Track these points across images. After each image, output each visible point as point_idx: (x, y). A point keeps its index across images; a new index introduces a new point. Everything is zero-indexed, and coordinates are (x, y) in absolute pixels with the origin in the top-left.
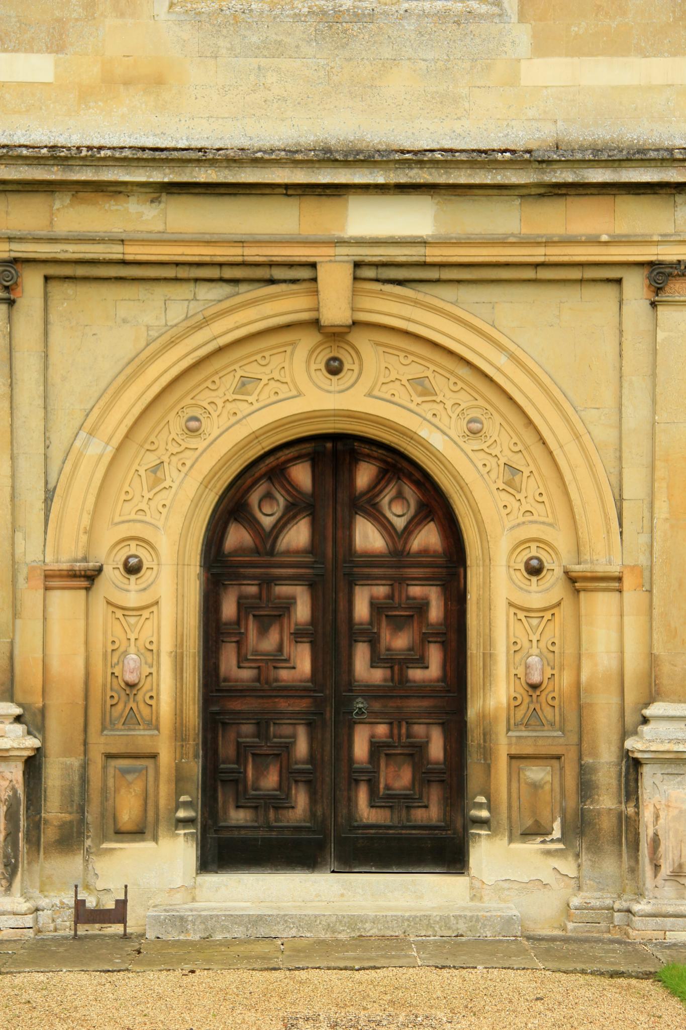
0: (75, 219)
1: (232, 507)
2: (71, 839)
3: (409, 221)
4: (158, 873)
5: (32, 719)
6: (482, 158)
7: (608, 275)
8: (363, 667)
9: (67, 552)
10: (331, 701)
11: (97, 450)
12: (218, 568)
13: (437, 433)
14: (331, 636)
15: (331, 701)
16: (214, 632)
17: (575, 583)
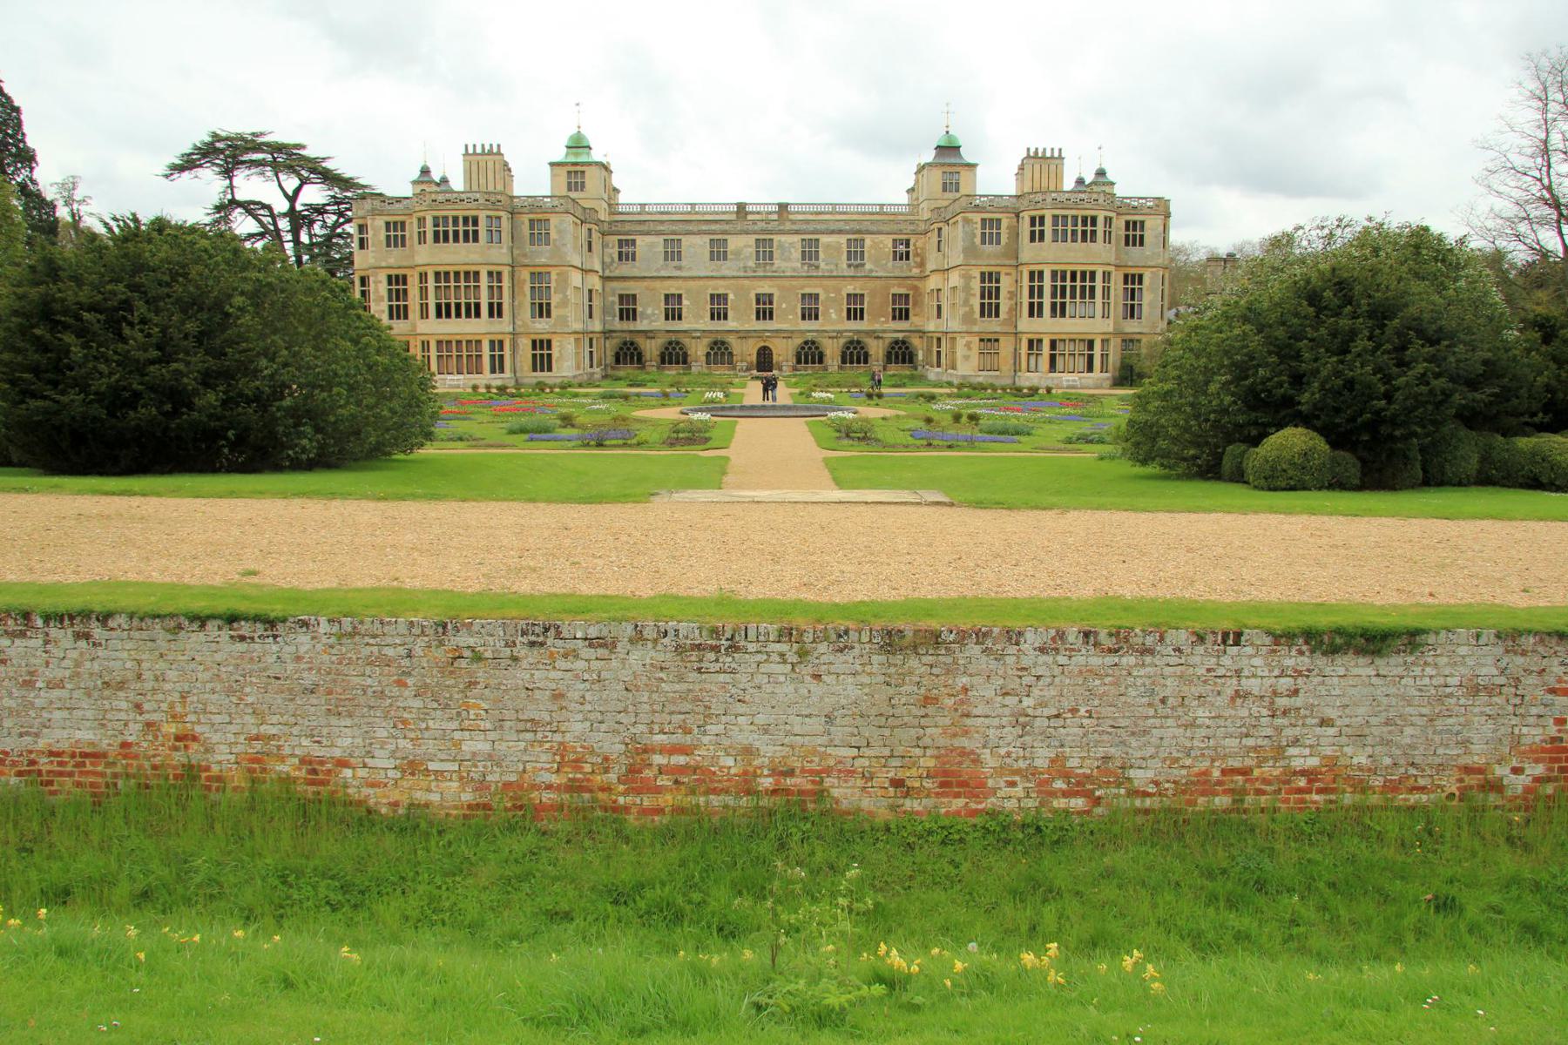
4: (755, 372)
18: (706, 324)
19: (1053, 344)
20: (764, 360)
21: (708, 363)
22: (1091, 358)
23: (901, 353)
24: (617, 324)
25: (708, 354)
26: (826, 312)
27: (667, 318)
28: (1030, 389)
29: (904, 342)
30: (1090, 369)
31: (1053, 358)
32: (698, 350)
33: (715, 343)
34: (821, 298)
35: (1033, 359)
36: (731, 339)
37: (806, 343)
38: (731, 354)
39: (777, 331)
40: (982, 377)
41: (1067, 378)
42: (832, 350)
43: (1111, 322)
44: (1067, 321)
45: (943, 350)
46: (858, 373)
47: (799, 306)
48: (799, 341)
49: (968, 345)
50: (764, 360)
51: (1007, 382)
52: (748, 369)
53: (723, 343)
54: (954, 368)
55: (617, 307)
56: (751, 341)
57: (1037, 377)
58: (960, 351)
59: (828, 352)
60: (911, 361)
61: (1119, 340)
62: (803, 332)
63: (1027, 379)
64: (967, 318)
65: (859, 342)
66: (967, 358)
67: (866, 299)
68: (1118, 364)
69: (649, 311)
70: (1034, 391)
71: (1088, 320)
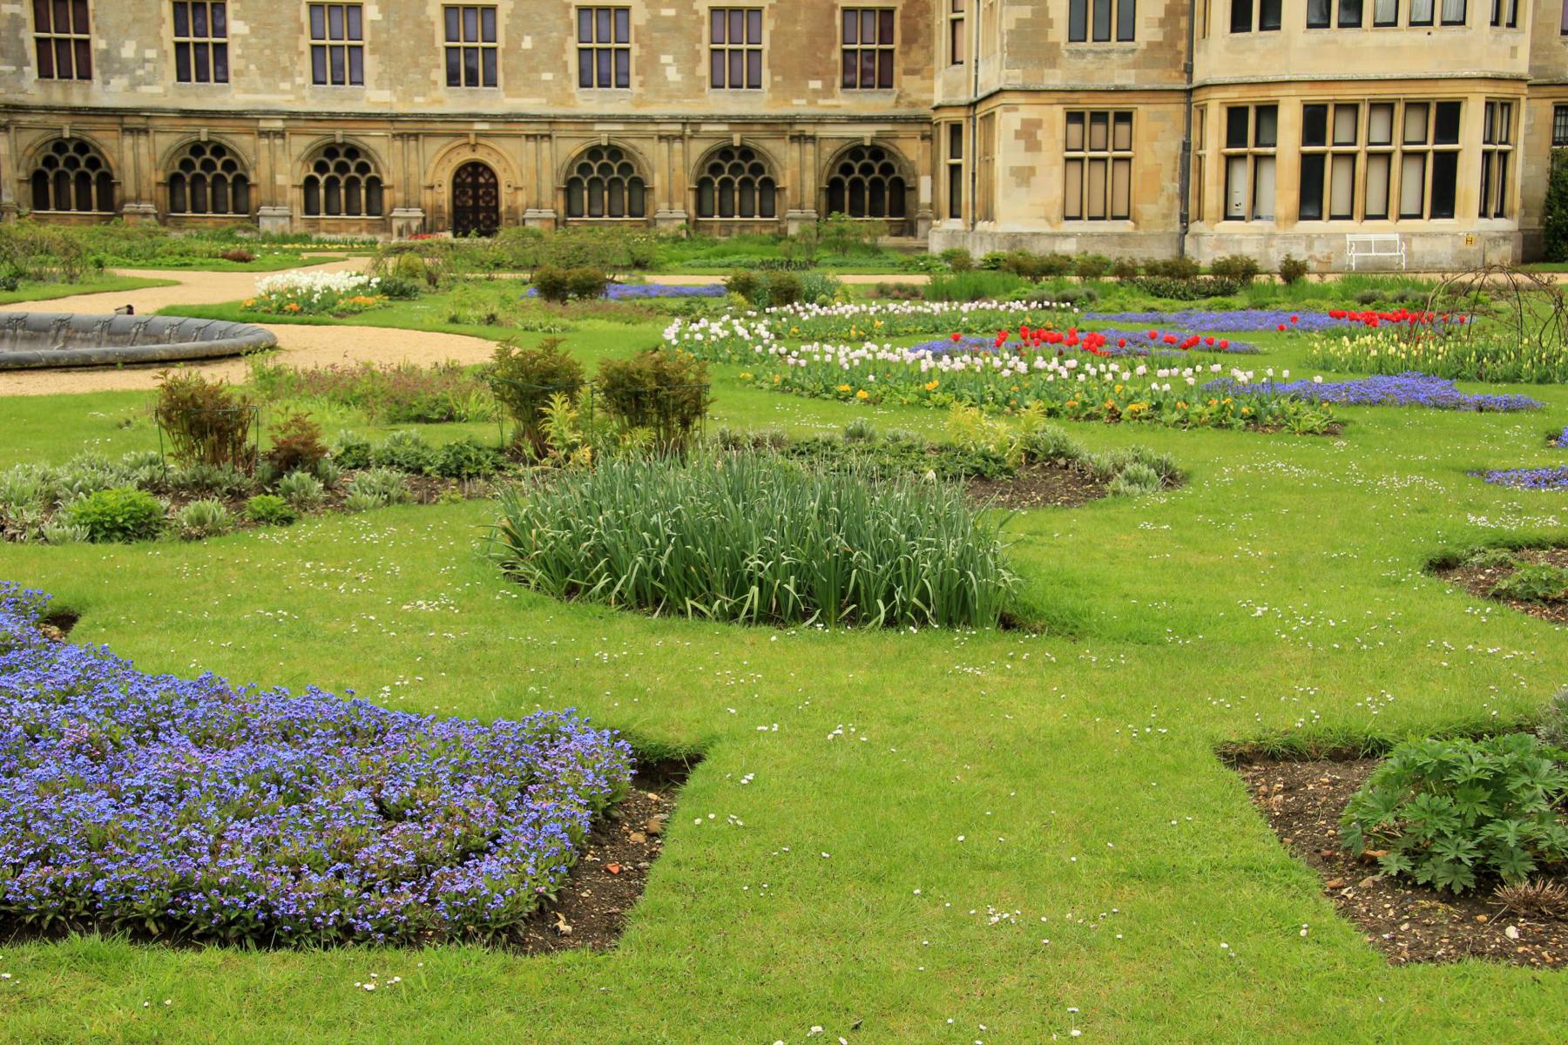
0: (428, 126)
1: (457, 174)
2: (431, 232)
3: (485, 127)
5: (424, 211)
6: (495, 116)
7: (519, 136)
8: (481, 203)
9: (428, 183)
10: (476, 209)
11: (433, 166)
12: (455, 185)
13: (492, 162)
14: (476, 197)
15: (476, 209)
16: (455, 197)
17: (517, 189)
18: (297, 92)
19: (1314, 122)
20: (475, 202)
21: (310, 208)
22: (1446, 166)
23: (869, 184)
24: (31, 89)
25: (310, 183)
26: (651, 64)
27: (183, 75)
28: (1221, 269)
29: (877, 152)
30: (1444, 204)
31: (1312, 170)
32: (280, 169)
33: (331, 151)
34: (638, 18)
35: (1242, 175)
36: (375, 141)
37: (594, 152)
38: (375, 185)
39: (508, 118)
40: (1071, 242)
41: (1356, 231)
42: (669, 171)
43: (1522, 39)
44: (1366, 37)
45: (965, 161)
46: (745, 245)
47: (572, 45)
48: (570, 147)
49: (1028, 135)
50: (475, 202)
51: (1162, 253)
52: (427, 228)
53: (353, 152)
54: (989, 216)
55: (29, 36)
56: (434, 147)
57: (1267, 235)
58: (1006, 153)
59: (657, 181)
60: (899, 208)
61: (1546, 108)
62: (584, 121)
63: (1215, 241)
64: (1028, 43)
65: (747, 153)
66: (1024, 176)
67: (768, 25)
68: (1541, 189)
69: (128, 51)
70: (1236, 274)
71: (1440, 34)
